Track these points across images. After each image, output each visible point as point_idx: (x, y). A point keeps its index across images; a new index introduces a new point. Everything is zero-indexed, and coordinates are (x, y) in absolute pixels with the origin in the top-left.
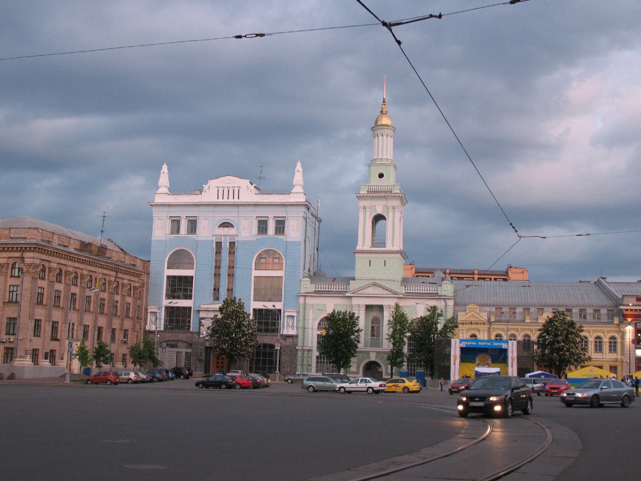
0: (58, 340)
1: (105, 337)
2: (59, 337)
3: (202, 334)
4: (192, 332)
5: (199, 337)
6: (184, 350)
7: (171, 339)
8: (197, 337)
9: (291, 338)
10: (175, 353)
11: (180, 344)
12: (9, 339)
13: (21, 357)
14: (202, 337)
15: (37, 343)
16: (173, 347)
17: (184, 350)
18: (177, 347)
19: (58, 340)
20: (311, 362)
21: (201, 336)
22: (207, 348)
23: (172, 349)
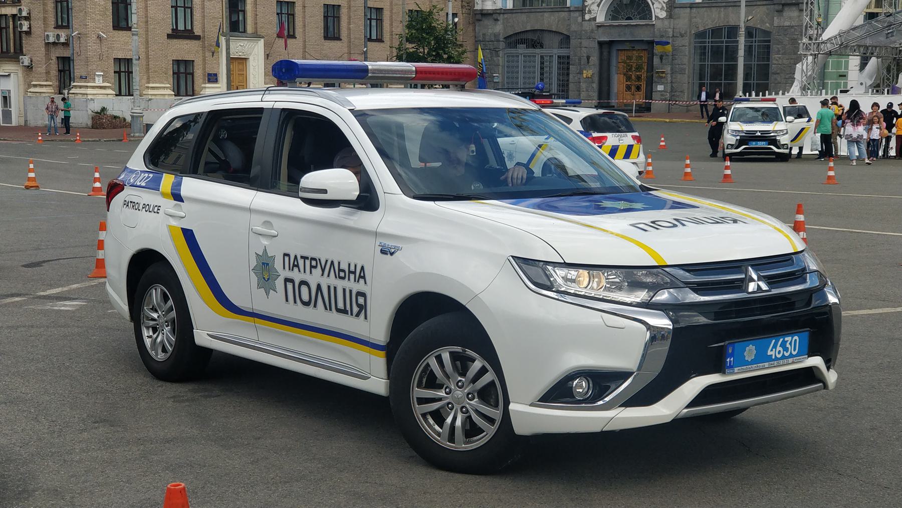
0: (198, 38)
1: (349, 29)
2: (197, 31)
3: (590, 12)
4: (569, 10)
5: (583, 19)
6: (556, 52)
7: (529, 28)
8: (580, 19)
9: (794, 8)
10: (538, 59)
11: (547, 39)
12: (58, 36)
13: (81, 77)
14: (590, 20)
15: (126, 44)
16: (534, 47)
17: (556, 52)
18: (542, 47)
19: (198, 38)
20: (847, 67)
21: (587, 17)
22: (601, 44)
23: (531, 50)
